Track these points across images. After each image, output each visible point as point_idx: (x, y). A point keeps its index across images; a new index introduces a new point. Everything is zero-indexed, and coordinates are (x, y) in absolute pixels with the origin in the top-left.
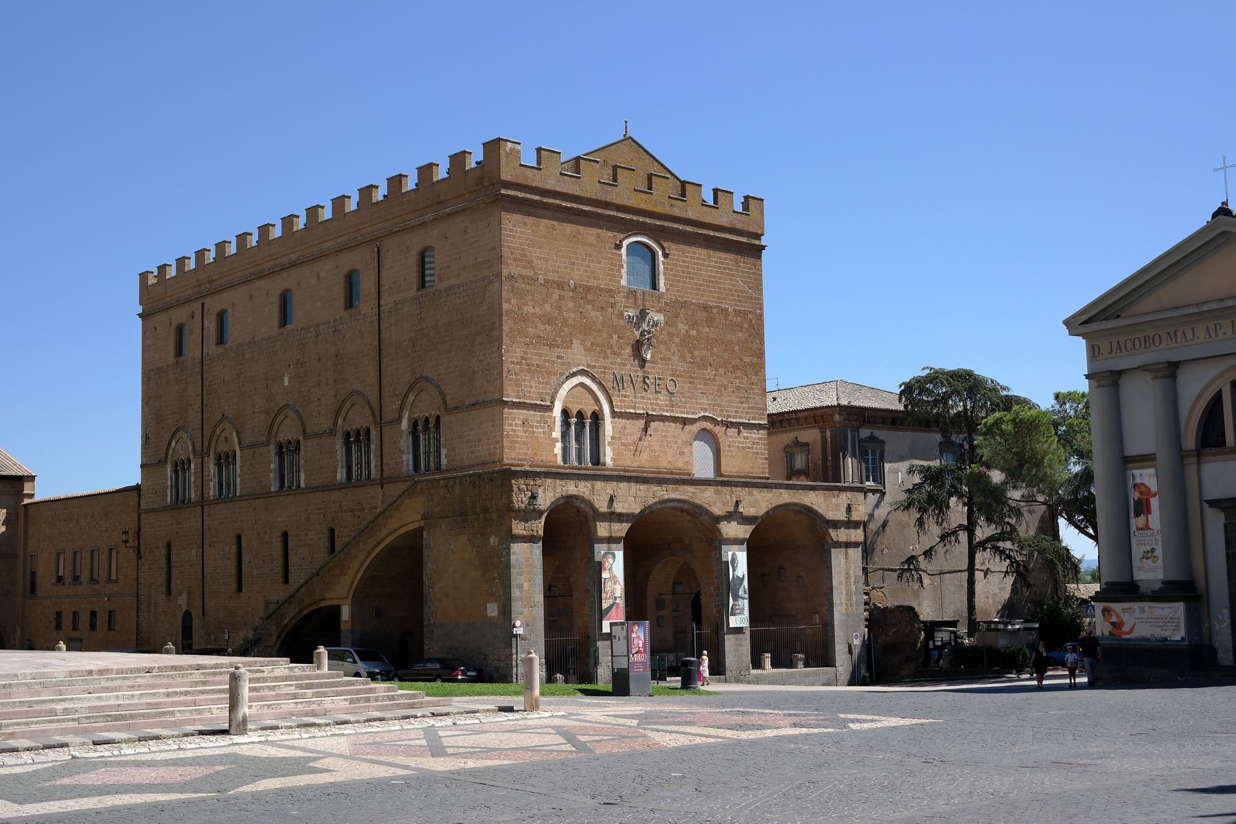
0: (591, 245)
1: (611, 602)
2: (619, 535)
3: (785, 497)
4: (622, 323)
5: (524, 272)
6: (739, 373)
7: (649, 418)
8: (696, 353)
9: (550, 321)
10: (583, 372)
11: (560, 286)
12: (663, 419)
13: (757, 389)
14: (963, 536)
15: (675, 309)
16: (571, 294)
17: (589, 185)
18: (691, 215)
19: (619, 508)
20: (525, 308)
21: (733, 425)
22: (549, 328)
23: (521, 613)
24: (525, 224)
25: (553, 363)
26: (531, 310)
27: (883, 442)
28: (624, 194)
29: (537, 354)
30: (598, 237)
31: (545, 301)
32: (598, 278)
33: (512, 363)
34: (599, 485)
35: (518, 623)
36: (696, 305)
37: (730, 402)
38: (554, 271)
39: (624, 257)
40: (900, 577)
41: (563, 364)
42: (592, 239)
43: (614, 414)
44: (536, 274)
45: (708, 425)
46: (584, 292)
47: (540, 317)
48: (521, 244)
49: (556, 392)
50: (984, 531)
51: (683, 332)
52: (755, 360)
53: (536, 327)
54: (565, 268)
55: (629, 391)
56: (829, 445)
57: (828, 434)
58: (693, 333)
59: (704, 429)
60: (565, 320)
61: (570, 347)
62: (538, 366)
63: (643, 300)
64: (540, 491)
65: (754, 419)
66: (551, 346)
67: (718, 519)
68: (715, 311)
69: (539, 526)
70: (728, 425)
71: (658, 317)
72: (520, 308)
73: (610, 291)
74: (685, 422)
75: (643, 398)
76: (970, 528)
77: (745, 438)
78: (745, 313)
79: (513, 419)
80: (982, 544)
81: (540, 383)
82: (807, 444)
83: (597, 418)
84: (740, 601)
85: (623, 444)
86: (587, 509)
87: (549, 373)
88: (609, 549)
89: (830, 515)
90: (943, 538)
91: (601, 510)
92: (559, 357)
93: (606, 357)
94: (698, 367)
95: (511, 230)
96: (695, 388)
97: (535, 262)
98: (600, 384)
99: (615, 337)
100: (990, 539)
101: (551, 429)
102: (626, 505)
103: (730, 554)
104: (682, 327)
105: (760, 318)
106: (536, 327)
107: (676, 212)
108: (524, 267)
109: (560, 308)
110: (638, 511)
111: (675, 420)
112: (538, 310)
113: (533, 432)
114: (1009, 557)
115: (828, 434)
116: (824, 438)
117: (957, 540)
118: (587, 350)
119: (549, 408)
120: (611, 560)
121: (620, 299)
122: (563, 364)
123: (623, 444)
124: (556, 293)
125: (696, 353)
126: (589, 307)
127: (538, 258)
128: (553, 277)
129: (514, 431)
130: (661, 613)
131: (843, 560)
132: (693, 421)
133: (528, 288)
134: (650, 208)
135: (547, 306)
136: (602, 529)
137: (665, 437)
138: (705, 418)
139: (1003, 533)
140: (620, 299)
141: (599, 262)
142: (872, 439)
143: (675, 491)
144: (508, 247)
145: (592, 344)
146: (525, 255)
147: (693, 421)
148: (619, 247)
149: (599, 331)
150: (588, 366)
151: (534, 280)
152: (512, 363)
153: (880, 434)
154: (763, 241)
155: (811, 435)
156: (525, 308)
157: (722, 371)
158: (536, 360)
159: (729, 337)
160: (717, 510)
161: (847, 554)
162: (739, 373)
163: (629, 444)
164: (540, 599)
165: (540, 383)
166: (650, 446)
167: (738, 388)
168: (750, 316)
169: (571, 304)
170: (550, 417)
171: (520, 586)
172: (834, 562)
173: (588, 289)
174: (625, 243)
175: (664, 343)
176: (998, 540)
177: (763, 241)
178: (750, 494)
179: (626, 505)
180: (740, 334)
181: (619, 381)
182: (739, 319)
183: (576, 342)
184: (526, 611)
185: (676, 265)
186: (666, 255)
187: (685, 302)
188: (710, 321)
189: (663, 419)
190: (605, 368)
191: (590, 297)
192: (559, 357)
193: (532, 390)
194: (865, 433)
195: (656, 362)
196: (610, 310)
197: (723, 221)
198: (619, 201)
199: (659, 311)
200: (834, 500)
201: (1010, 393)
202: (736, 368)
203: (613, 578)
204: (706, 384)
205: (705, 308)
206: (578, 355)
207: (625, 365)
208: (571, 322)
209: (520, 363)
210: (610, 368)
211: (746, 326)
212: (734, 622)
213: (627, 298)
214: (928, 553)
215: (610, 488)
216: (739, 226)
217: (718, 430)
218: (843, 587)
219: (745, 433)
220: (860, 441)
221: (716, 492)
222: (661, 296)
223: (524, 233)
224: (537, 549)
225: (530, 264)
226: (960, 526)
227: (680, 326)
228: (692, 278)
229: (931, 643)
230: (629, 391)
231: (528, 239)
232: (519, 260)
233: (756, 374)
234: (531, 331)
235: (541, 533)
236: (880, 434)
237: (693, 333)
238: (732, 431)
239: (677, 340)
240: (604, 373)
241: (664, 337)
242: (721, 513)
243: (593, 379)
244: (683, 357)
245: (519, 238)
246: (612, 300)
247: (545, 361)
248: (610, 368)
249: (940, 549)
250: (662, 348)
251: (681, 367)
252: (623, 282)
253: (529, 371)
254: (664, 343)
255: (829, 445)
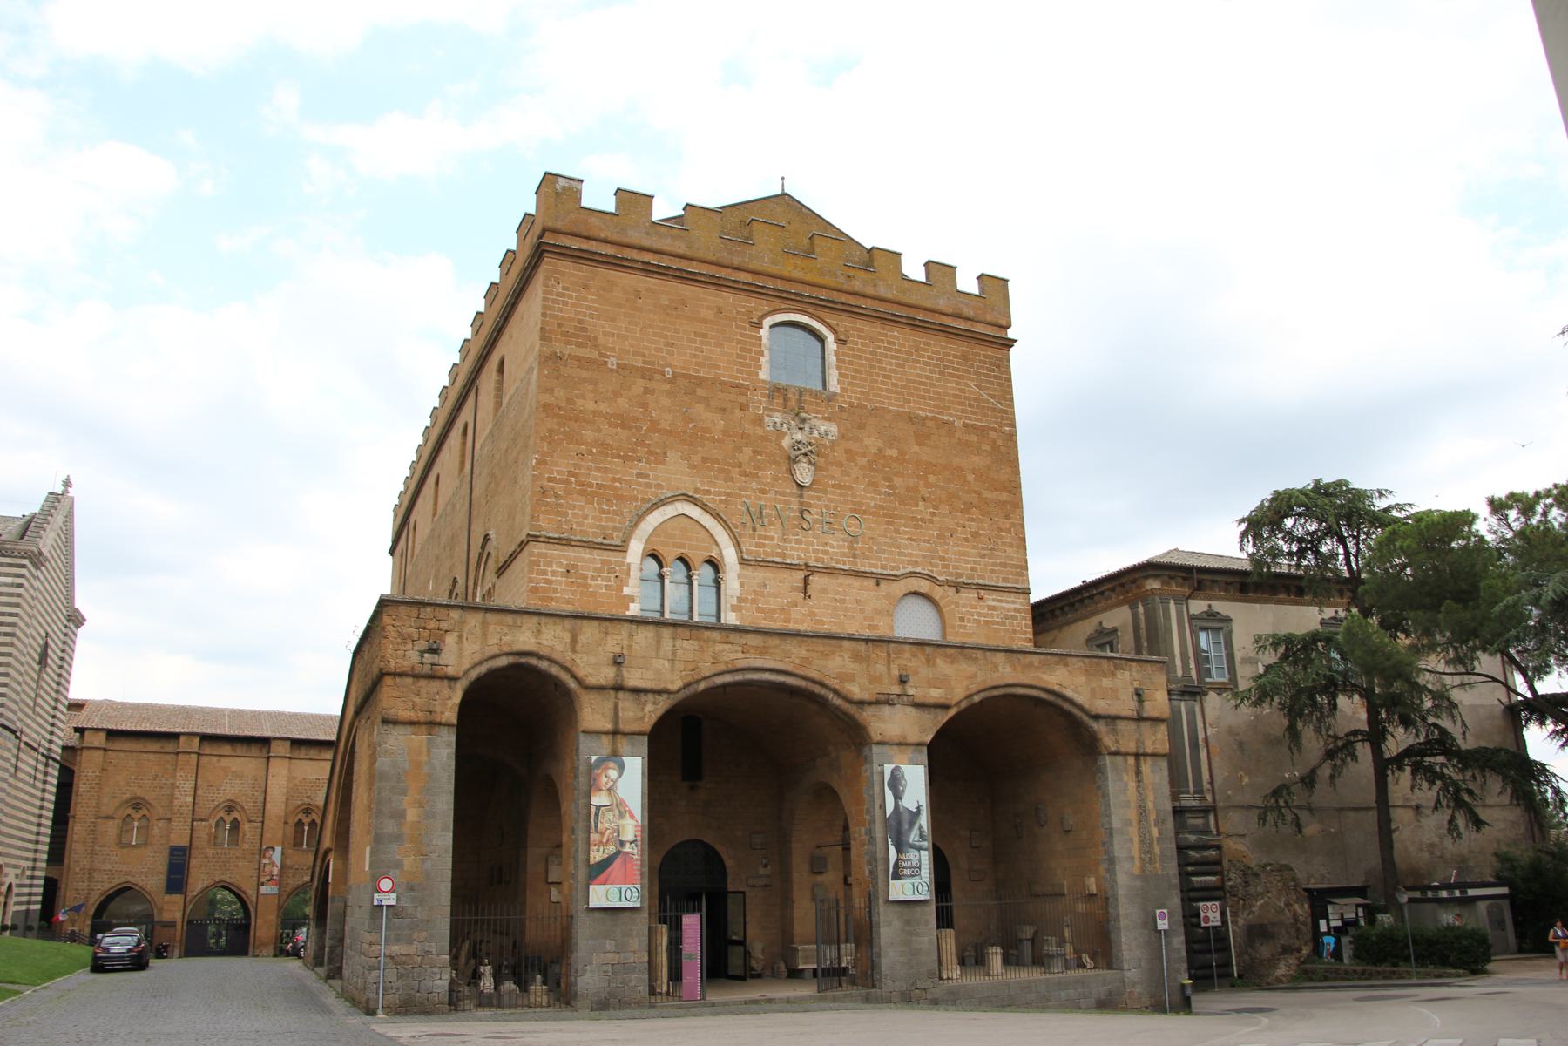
0: (705, 321)
1: (611, 849)
2: (635, 727)
3: (1005, 673)
4: (759, 431)
5: (581, 352)
6: (975, 513)
7: (810, 570)
8: (898, 481)
9: (624, 422)
10: (686, 498)
11: (647, 373)
12: (832, 572)
13: (1008, 538)
14: (1364, 751)
15: (855, 417)
16: (668, 386)
17: (706, 243)
18: (883, 291)
19: (633, 679)
20: (580, 402)
21: (967, 586)
22: (623, 434)
23: (398, 865)
24: (585, 287)
25: (629, 483)
26: (590, 406)
27: (1228, 620)
28: (764, 254)
29: (598, 469)
30: (719, 311)
31: (617, 394)
32: (718, 367)
33: (550, 479)
34: (589, 632)
35: (386, 884)
36: (899, 415)
37: (961, 553)
38: (635, 354)
39: (765, 341)
40: (1262, 819)
41: (649, 486)
42: (710, 315)
43: (743, 562)
44: (601, 355)
45: (924, 586)
46: (691, 385)
47: (607, 416)
48: (577, 313)
49: (636, 525)
50: (1398, 739)
51: (874, 450)
52: (1005, 497)
53: (599, 430)
54: (657, 350)
55: (775, 532)
56: (1143, 625)
57: (1141, 609)
58: (893, 453)
59: (916, 593)
60: (654, 426)
61: (663, 462)
62: (599, 486)
63: (800, 401)
64: (450, 639)
65: (1005, 580)
66: (625, 459)
67: (861, 703)
68: (930, 424)
69: (449, 704)
70: (958, 587)
71: (833, 428)
72: (569, 401)
73: (737, 386)
74: (879, 579)
75: (798, 541)
76: (1376, 735)
77: (990, 608)
78: (983, 431)
79: (549, 564)
80: (1398, 761)
81: (602, 511)
82: (1114, 631)
83: (714, 564)
84: (912, 855)
85: (759, 610)
86: (564, 676)
87: (619, 498)
88: (615, 753)
89: (1100, 706)
90: (1330, 754)
91: (592, 681)
92: (639, 475)
93: (732, 479)
94: (902, 502)
95: (562, 295)
96: (897, 531)
97: (601, 340)
98: (717, 516)
99: (748, 451)
100: (1408, 752)
101: (621, 581)
102: (650, 675)
103: (888, 769)
104: (872, 443)
105: (1012, 437)
106: (599, 430)
107: (857, 285)
108: (580, 345)
109: (645, 405)
110: (678, 684)
111: (859, 574)
112: (603, 407)
113: (586, 586)
114: (1442, 776)
115: (1141, 609)
116: (1135, 617)
117: (1355, 758)
118: (692, 467)
119: (622, 548)
120: (613, 774)
121: (758, 400)
122: (649, 486)
123: (759, 610)
124: (639, 385)
125: (898, 481)
126: (700, 407)
127: (606, 334)
128: (630, 360)
129: (547, 581)
130: (820, 878)
131: (1132, 785)
132: (896, 578)
133: (584, 374)
134: (809, 277)
135: (620, 401)
136: (593, 714)
137: (843, 601)
138: (914, 574)
139: (1428, 742)
140: (758, 400)
141: (721, 346)
142: (1211, 615)
143: (763, 651)
144: (555, 317)
145: (704, 460)
146: (585, 330)
147: (896, 578)
148: (759, 325)
149: (720, 441)
150: (697, 490)
151: (598, 365)
152: (550, 479)
153: (1221, 607)
154: (1011, 334)
155: (1118, 617)
156: (580, 402)
157: (945, 509)
158: (595, 478)
159: (956, 461)
160: (856, 690)
161: (1138, 772)
162: (975, 513)
163: (773, 611)
164: (443, 839)
165: (602, 511)
166: (812, 614)
167: (975, 535)
168: (992, 435)
169: (666, 402)
170: (622, 564)
171: (403, 815)
172: (1112, 787)
173: (700, 381)
174: (768, 322)
175: (840, 465)
176: (1423, 754)
177: (1011, 334)
178: (930, 662)
179: (650, 675)
180: (976, 459)
181: (757, 516)
182: (974, 438)
183: (673, 456)
184: (409, 863)
185: (860, 357)
186: (839, 341)
187: (876, 409)
188: (921, 439)
189: (832, 572)
190: (729, 495)
191: (700, 392)
192: (639, 475)
193: (587, 519)
194: (1198, 606)
195: (825, 492)
196: (738, 413)
197: (942, 304)
198: (754, 265)
199: (829, 419)
200: (1106, 682)
201: (1414, 510)
202: (969, 506)
203: (621, 808)
204: (917, 527)
205: (912, 418)
206: (675, 471)
207: (764, 492)
208: (664, 425)
209: (567, 481)
210: (740, 496)
211: (988, 448)
212: (900, 890)
213: (771, 397)
214: (1309, 780)
215: (615, 640)
216: (967, 312)
217: (938, 592)
218: (1133, 831)
219: (990, 598)
220: (1192, 618)
221: (857, 657)
222: (832, 398)
223: (585, 299)
224: (443, 751)
225: (592, 341)
226: (1355, 733)
227: (867, 441)
228: (889, 377)
229: (1323, 923)
230: (775, 532)
231: (588, 308)
232: (573, 335)
233: (1008, 517)
234: (589, 435)
235: (451, 716)
236: (1221, 607)
237: (893, 453)
238: (966, 595)
239: (862, 461)
240: (726, 502)
241: (839, 454)
242: (866, 696)
243: (705, 508)
244: (873, 485)
245: (573, 305)
246: (742, 399)
247: (614, 480)
248: (740, 496)
249: (1325, 771)
250: (835, 471)
251: (871, 499)
252: (763, 375)
253: (582, 493)
254: (840, 465)
255: (1143, 625)
